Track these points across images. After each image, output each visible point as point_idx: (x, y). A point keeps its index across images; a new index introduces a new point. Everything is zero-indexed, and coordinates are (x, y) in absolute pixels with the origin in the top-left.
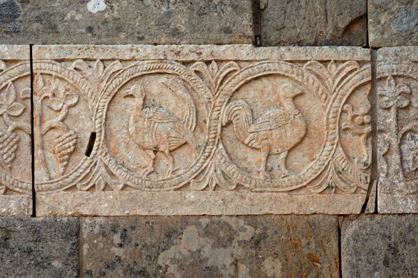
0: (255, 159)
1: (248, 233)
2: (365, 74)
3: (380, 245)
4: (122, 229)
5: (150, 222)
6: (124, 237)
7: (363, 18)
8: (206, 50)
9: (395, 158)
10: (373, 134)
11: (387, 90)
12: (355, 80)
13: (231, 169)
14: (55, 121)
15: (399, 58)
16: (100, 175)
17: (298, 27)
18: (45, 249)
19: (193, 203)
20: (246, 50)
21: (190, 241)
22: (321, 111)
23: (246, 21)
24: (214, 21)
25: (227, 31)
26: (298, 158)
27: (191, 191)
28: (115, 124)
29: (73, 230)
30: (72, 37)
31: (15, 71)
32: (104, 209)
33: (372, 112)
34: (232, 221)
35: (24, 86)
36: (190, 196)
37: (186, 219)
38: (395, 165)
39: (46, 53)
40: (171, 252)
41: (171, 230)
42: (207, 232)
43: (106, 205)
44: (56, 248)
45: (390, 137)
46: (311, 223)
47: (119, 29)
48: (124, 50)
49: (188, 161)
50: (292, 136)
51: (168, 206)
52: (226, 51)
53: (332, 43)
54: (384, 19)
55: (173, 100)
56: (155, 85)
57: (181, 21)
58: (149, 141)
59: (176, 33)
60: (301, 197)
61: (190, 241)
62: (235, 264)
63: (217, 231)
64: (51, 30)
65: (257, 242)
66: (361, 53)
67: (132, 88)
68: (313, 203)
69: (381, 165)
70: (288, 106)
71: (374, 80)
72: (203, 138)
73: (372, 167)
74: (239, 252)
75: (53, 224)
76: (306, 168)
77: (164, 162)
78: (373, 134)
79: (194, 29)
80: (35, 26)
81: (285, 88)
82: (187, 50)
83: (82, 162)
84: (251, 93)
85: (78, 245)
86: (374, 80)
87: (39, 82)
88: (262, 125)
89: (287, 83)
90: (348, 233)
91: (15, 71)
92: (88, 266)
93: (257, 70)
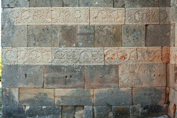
0: (113, 19)
1: (112, 26)
2: (124, 11)
3: (125, 28)
4: (99, 26)
5: (102, 25)
6: (99, 27)
7: (124, 5)
8: (108, 8)
9: (127, 19)
10: (125, 17)
11: (127, 12)
12: (124, 11)
13: (110, 20)
14: (92, 15)
15: (128, 9)
16: (97, 21)
17: (117, 6)
18: (91, 28)
19: (107, 23)
20: (112, 8)
21: (106, 27)
22: (120, 14)
23: (112, 5)
24: (109, 5)
25: (110, 6)
26: (117, 19)
27: (107, 22)
28: (98, 15)
29: (94, 26)
30: (94, 6)
31: (88, 10)
32: (97, 24)
33: (125, 14)
34: (111, 26)
35: (89, 11)
36: (106, 23)
37: (106, 25)
38: (127, 20)
39: (91, 8)
40: (104, 28)
41: (104, 26)
42: (108, 26)
43: (97, 24)
44: (92, 28)
45: (127, 17)
46: (119, 26)
47: (99, 6)
48: (99, 8)
49: (106, 19)
50: (117, 17)
51: (104, 24)
52: (110, 8)
53: (121, 7)
54: (126, 5)
55: (105, 13)
56: (103, 11)
57: (106, 5)
58: (102, 17)
59: (105, 6)
60: (118, 23)
61: (106, 27)
62: (111, 30)
63: (109, 26)
64: (92, 5)
65: (113, 27)
66: (124, 8)
67: (101, 12)
68: (119, 23)
69: (126, 20)
70: (117, 14)
71: (125, 11)
72: (108, 17)
73: (125, 20)
74: (111, 28)
75: (92, 26)
76: (118, 20)
77: (104, 19)
78: (125, 17)
79: (107, 6)
80: (90, 5)
81: (116, 12)
82: (106, 8)
83: (95, 19)
84: (113, 12)
85: (94, 28)
86: (125, 11)
87: (90, 11)
88: (114, 16)
89: (116, 11)
90: (122, 26)
91: (88, 10)
92: (95, 30)
93: (113, 10)
